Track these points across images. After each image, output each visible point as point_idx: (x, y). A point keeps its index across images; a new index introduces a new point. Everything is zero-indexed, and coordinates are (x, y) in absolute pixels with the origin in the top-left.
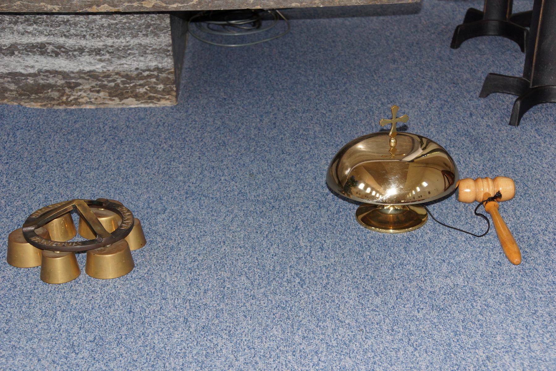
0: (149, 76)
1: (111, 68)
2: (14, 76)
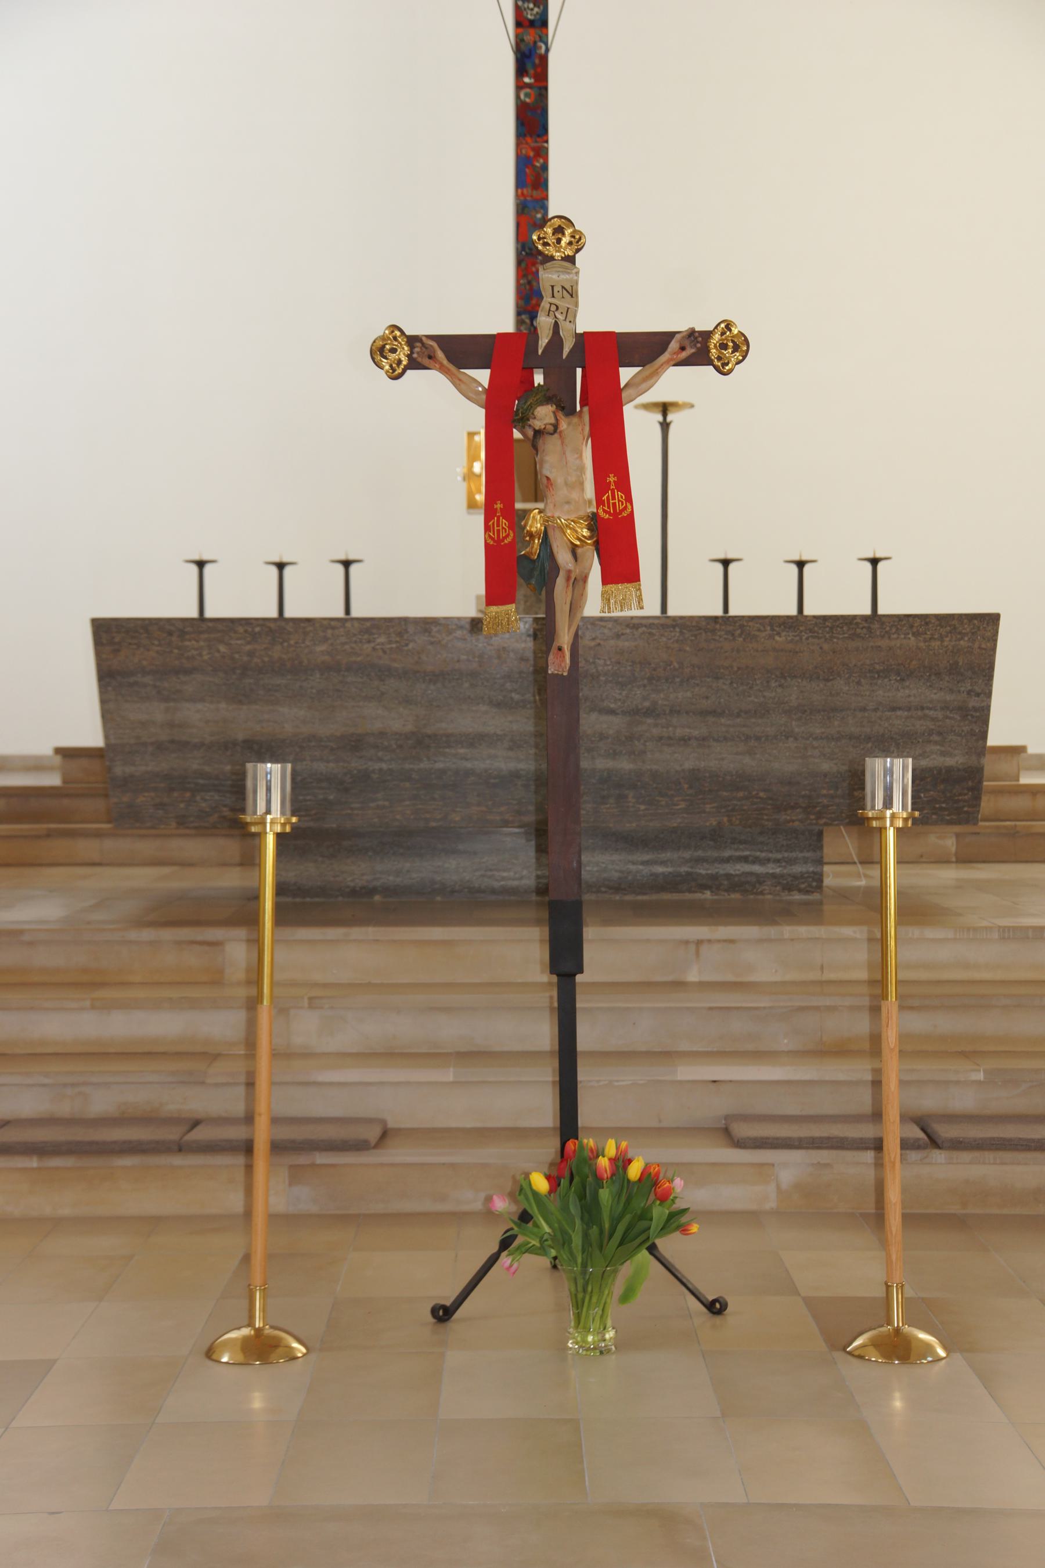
0: (808, 877)
1: (785, 871)
2: (728, 876)
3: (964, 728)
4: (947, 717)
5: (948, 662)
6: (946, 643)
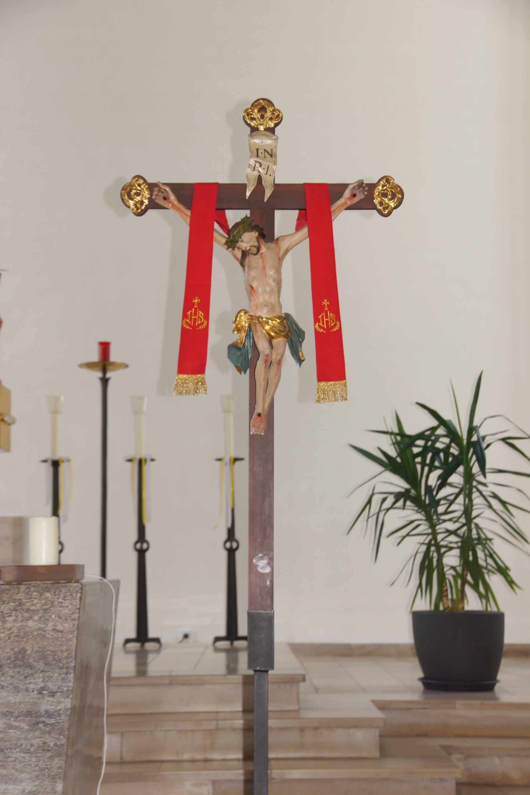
3: (34, 742)
4: (11, 727)
5: (12, 650)
6: (9, 625)
